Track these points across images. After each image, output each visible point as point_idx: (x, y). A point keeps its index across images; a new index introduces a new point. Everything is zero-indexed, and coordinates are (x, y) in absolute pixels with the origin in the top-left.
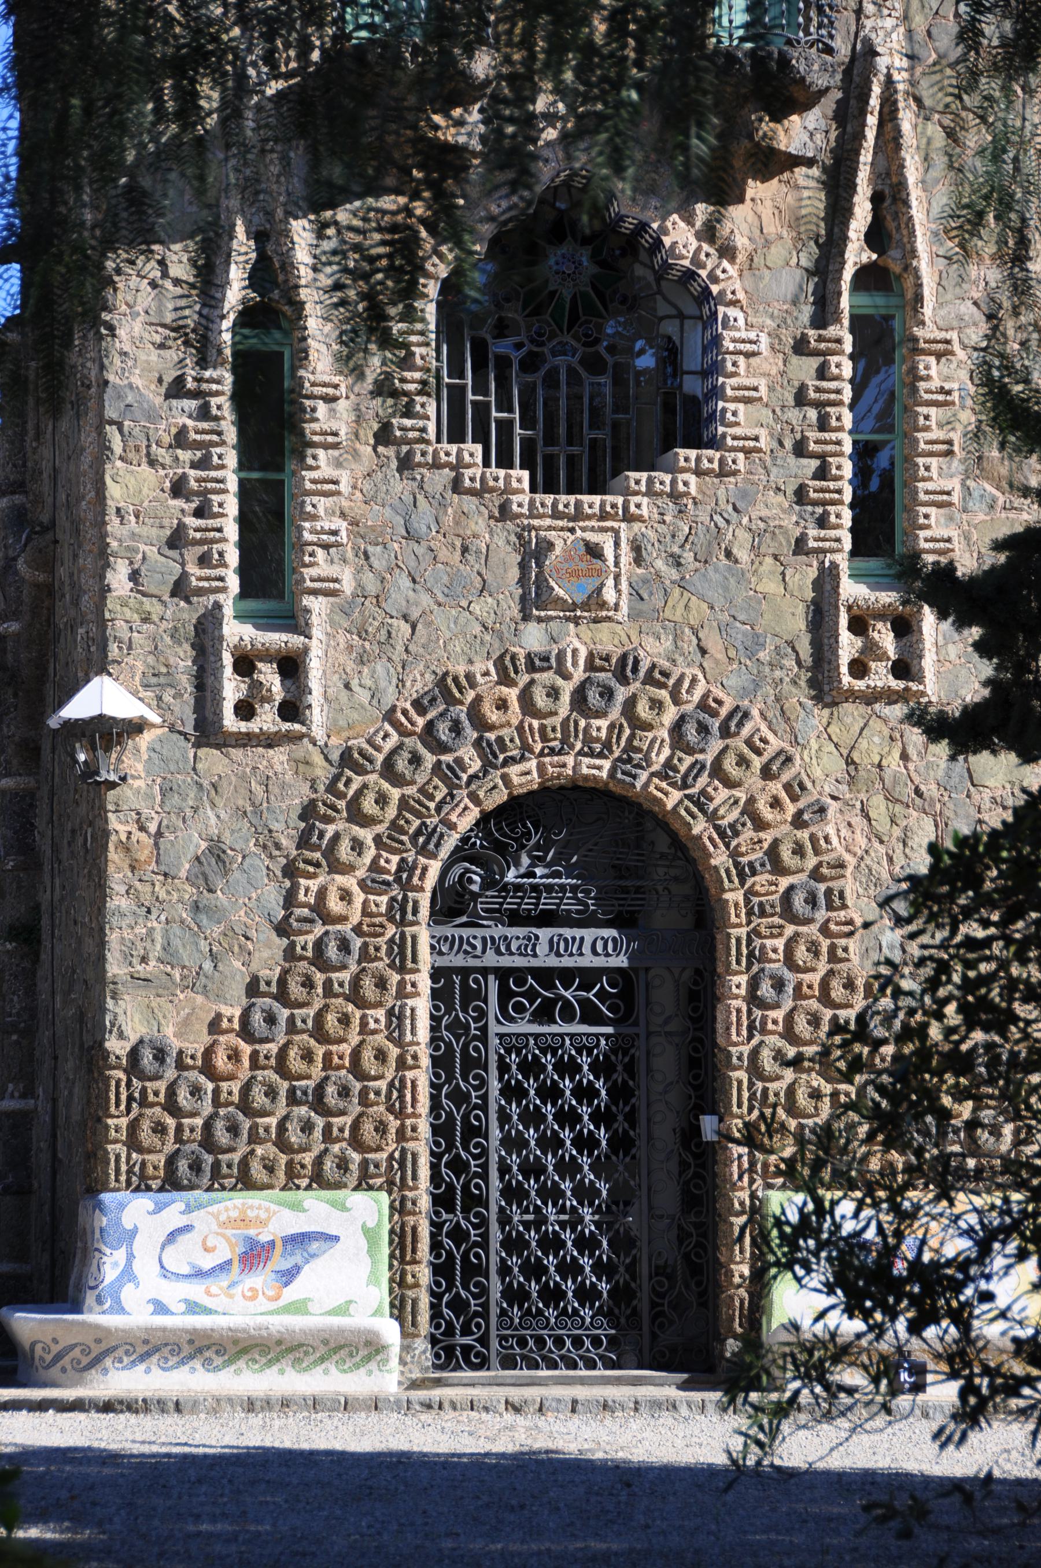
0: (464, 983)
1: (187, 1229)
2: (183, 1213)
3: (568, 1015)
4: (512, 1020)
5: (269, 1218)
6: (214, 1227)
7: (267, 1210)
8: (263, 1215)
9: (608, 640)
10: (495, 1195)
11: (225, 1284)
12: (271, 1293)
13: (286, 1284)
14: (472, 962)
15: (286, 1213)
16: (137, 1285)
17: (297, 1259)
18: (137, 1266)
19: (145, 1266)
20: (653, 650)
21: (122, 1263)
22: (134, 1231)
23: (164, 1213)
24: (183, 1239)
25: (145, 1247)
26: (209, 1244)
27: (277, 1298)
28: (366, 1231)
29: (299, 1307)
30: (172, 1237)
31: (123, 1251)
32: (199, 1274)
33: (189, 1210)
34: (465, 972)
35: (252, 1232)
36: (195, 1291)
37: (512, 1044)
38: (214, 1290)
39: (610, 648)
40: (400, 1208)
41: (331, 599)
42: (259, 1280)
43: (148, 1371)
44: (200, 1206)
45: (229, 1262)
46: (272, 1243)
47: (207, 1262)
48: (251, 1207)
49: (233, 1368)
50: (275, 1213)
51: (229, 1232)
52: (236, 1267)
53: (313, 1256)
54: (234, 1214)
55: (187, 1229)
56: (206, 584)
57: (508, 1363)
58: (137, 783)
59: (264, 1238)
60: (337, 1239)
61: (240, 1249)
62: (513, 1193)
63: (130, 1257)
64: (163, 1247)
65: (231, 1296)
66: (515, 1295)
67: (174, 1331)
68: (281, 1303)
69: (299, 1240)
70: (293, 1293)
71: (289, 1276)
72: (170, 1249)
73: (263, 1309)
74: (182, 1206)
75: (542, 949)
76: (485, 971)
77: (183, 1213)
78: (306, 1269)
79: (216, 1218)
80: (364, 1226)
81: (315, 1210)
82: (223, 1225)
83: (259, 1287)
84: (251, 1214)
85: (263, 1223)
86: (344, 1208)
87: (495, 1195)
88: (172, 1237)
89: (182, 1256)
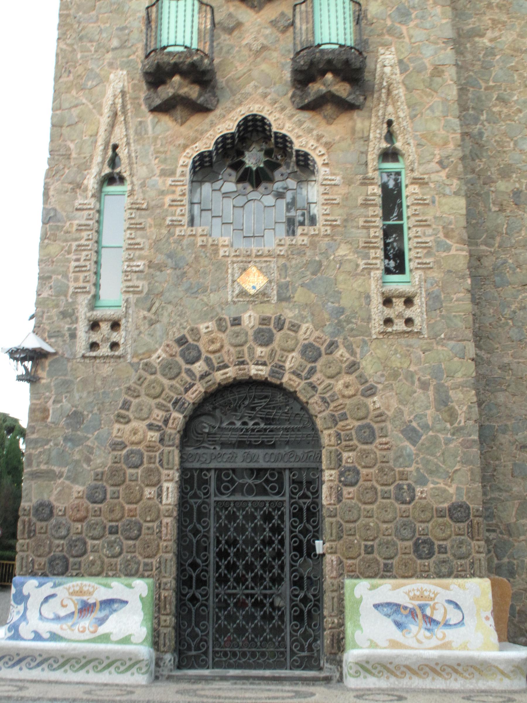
0: (199, 475)
1: (53, 596)
2: (52, 587)
3: (250, 491)
4: (222, 494)
5: (94, 591)
6: (67, 595)
7: (93, 587)
8: (91, 590)
9: (269, 311)
10: (212, 580)
11: (70, 624)
12: (92, 629)
13: (101, 625)
14: (204, 466)
15: (102, 589)
16: (27, 623)
17: (106, 612)
18: (28, 613)
19: (33, 615)
20: (289, 314)
21: (22, 612)
22: (28, 596)
23: (43, 587)
24: (51, 600)
25: (33, 603)
26: (65, 603)
27: (95, 632)
28: (141, 598)
29: (105, 638)
30: (46, 599)
31: (23, 605)
32: (58, 618)
33: (55, 586)
34: (202, 470)
35: (85, 598)
36: (55, 627)
37: (224, 506)
38: (64, 626)
39: (268, 315)
40: (159, 587)
41: (137, 296)
42: (87, 622)
43: (21, 669)
44: (60, 584)
45: (73, 613)
46: (95, 604)
47: (62, 613)
48: (85, 585)
49: (63, 669)
50: (98, 589)
51: (74, 598)
52: (76, 615)
53: (115, 611)
54: (77, 589)
55: (53, 596)
56: (79, 290)
57: (217, 665)
58: (43, 381)
59: (91, 601)
60: (126, 602)
61: (79, 606)
62: (222, 580)
63: (26, 609)
64: (42, 604)
65: (73, 630)
66: (221, 631)
67: (33, 650)
68: (97, 634)
69: (109, 603)
70: (103, 629)
71: (102, 621)
72: (45, 606)
73: (87, 637)
74: (51, 584)
75: (239, 458)
76: (209, 470)
77: (52, 587)
78: (111, 617)
79: (67, 591)
80: (140, 596)
81: (117, 588)
82: (71, 594)
83: (87, 626)
84: (85, 589)
85: (90, 593)
86: (129, 586)
87: (212, 580)
88: (46, 599)
89: (48, 611)
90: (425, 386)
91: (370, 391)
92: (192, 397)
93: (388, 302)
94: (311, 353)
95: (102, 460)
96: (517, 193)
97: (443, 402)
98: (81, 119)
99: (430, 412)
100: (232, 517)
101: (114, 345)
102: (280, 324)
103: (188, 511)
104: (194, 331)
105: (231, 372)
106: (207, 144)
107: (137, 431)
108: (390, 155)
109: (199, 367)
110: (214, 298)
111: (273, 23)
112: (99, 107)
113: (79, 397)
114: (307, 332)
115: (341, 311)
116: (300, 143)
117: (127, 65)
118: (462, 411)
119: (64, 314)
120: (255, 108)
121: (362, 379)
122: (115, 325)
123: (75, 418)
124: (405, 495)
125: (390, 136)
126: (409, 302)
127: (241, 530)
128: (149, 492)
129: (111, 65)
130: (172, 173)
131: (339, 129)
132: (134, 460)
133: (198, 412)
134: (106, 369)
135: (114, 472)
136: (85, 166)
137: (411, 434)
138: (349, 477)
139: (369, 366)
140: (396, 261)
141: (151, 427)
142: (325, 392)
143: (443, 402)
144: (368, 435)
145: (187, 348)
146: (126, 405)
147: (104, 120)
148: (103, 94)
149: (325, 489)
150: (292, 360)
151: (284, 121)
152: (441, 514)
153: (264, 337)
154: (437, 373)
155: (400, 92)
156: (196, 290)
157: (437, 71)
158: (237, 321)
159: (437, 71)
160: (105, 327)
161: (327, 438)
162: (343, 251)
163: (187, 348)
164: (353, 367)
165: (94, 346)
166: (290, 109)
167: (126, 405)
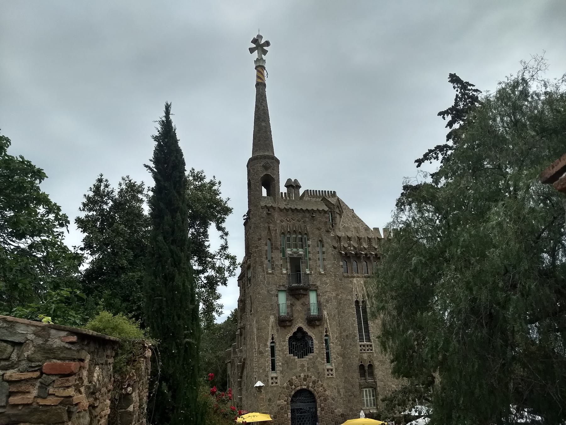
20: (310, 374)
90: (335, 389)
91: (325, 391)
92: (293, 393)
93: (328, 370)
94: (314, 382)
95: (276, 409)
96: (347, 336)
97: (339, 392)
98: (265, 328)
99: (337, 394)
100: (300, 419)
101: (276, 383)
102: (308, 376)
103: (293, 419)
104: (292, 379)
105: (299, 388)
106: (290, 334)
107: (282, 402)
108: (326, 336)
109: (293, 387)
110: (295, 371)
111: (302, 304)
112: (269, 325)
113: (270, 395)
114: (313, 378)
115: (319, 373)
116: (310, 334)
117: (274, 314)
118: (342, 394)
119: (266, 376)
120: (300, 325)
121: (324, 388)
122: (276, 378)
123: (270, 400)
124: (333, 412)
125: (326, 332)
126: (332, 370)
127: (302, 421)
128: (286, 415)
129: (271, 315)
130: (285, 341)
131: (316, 330)
132: (282, 408)
133: (294, 396)
134: (275, 388)
135: (279, 412)
136: (267, 340)
137: (333, 399)
138: (322, 409)
139: (325, 385)
140: (328, 361)
141: (285, 401)
142: (318, 391)
143: (339, 392)
144: (325, 400)
145: (291, 383)
146: (280, 397)
147: (270, 328)
148: (269, 322)
149: (318, 412)
150: (311, 384)
151: (306, 329)
152: (339, 416)
153: (305, 379)
154: (337, 386)
155: (328, 321)
156: (291, 369)
157: (335, 316)
158: (300, 376)
159: (335, 316)
160: (274, 379)
161: (318, 401)
162: (319, 359)
163: (291, 383)
164: (322, 385)
165: (272, 383)
166: (307, 326)
167: (280, 397)
